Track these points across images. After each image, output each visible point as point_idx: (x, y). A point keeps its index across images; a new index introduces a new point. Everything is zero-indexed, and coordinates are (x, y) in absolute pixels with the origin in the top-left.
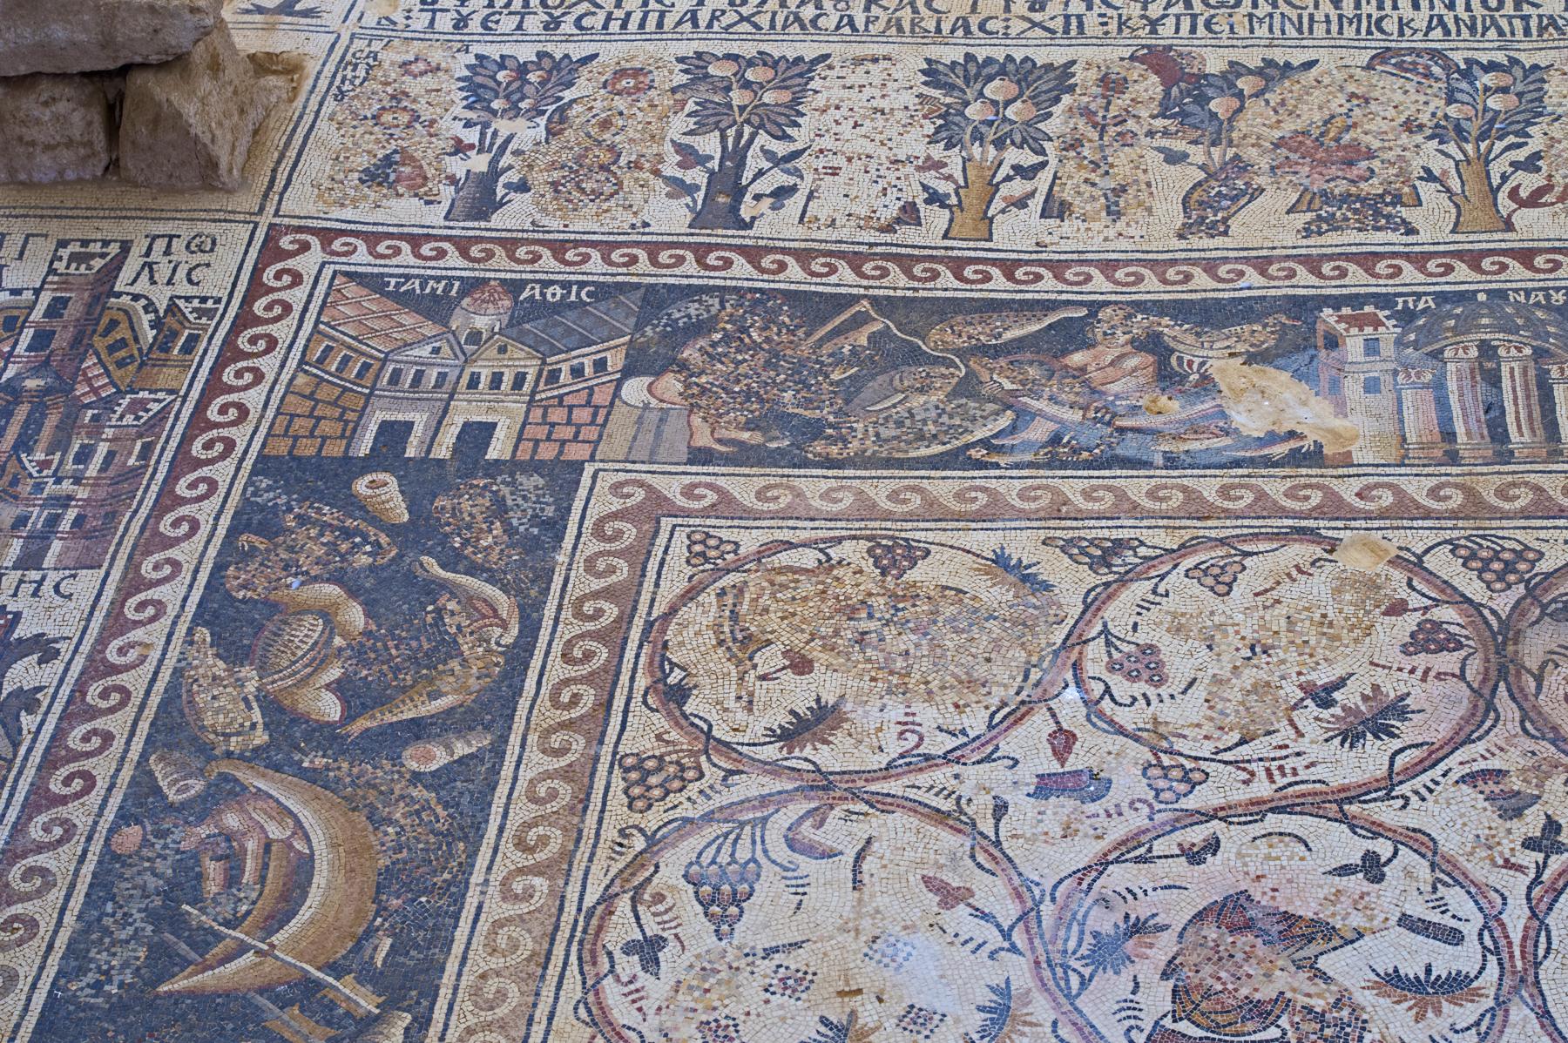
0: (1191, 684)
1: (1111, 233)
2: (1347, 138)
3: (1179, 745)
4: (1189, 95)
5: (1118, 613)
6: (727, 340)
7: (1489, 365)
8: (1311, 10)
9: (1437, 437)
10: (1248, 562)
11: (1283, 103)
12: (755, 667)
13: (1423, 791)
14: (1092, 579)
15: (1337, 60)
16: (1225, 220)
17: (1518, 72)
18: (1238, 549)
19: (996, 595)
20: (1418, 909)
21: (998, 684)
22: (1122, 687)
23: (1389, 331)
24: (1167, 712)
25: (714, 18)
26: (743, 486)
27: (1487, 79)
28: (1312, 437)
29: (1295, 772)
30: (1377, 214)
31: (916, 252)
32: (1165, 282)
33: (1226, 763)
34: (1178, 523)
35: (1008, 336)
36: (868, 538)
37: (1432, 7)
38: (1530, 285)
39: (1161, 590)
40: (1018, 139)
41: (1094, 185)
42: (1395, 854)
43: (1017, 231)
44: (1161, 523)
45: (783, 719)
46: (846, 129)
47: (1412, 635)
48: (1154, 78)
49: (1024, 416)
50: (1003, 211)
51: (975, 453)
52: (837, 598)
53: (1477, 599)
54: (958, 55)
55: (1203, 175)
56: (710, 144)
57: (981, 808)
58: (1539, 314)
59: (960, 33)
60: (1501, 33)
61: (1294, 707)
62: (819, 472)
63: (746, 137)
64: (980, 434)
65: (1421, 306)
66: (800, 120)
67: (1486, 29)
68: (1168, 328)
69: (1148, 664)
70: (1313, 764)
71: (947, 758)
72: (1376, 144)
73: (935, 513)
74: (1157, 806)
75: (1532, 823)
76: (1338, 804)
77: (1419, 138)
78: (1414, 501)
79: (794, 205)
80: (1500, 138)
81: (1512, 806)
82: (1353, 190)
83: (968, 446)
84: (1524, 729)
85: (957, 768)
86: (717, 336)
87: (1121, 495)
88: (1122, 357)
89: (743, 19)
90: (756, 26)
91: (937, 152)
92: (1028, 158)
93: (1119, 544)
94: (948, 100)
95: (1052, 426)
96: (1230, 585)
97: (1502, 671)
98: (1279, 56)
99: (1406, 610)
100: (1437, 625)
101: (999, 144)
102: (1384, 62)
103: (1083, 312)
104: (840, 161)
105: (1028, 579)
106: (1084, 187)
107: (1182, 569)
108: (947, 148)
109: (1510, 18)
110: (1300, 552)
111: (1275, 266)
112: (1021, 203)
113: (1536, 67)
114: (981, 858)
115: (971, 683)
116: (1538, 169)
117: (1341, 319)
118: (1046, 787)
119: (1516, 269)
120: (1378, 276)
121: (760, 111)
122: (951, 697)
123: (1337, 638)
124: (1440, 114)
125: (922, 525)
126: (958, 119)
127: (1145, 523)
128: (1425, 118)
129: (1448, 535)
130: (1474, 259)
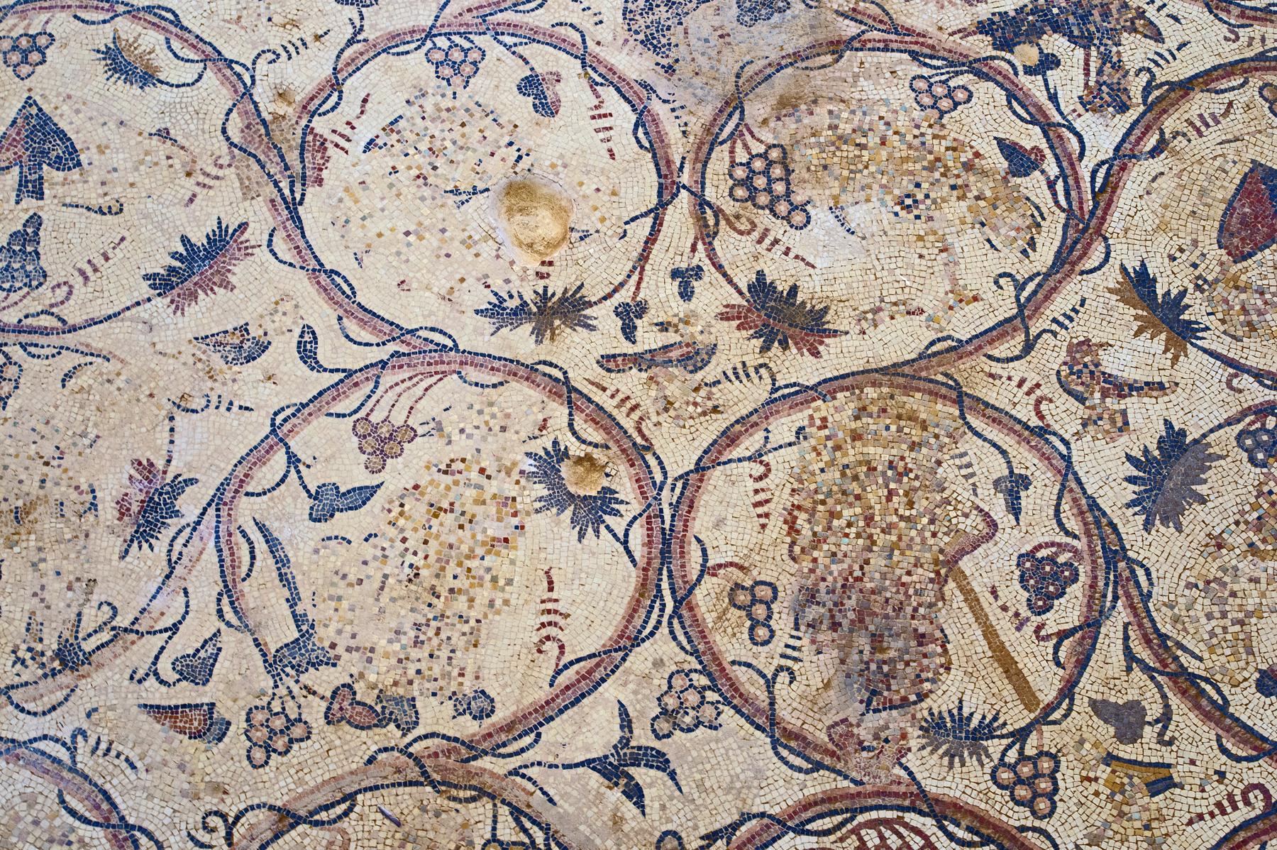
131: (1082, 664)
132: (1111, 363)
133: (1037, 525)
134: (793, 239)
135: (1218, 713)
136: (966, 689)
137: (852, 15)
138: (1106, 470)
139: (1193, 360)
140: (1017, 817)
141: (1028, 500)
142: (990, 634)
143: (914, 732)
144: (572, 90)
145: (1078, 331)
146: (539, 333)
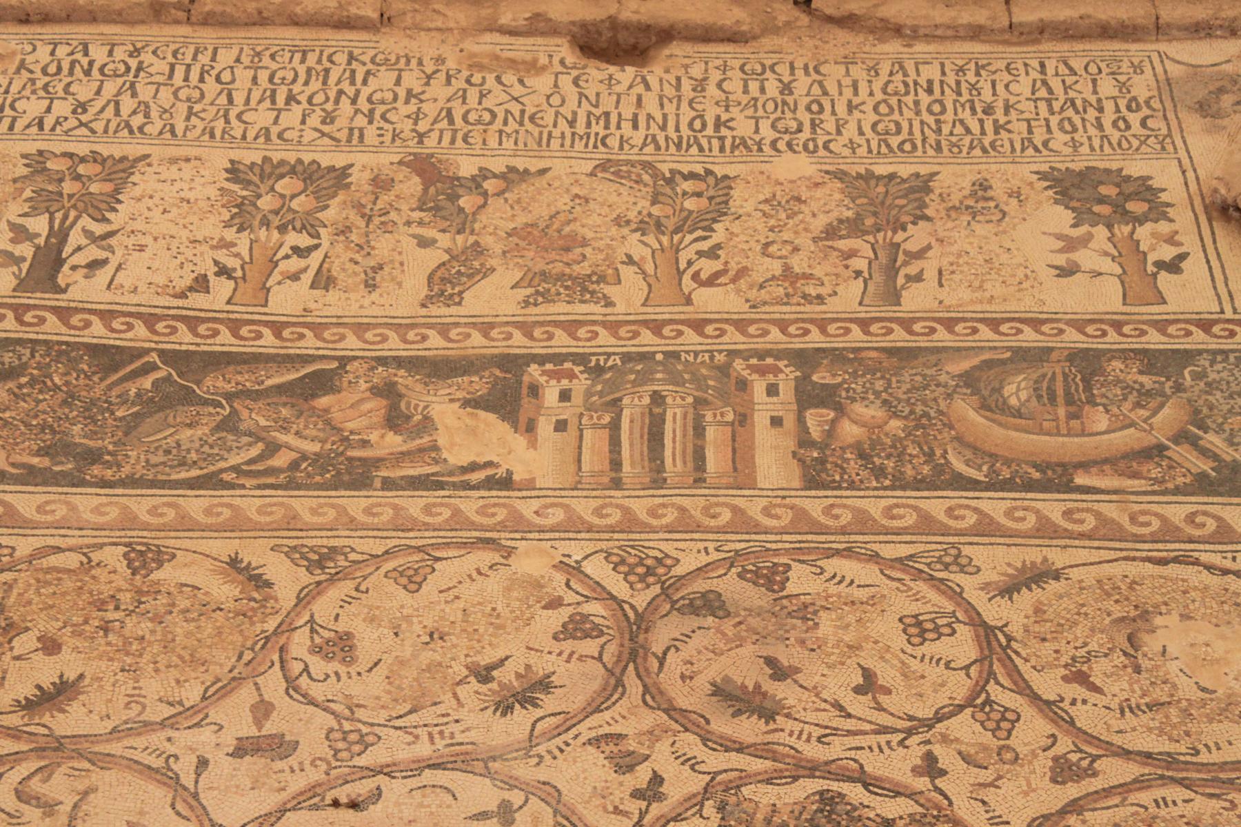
0: (376, 664)
1: (366, 302)
2: (567, 229)
3: (360, 714)
4: (442, 191)
5: (323, 608)
6: (33, 381)
7: (657, 410)
8: (550, 128)
9: (606, 466)
10: (438, 566)
11: (519, 201)
12: (11, 649)
13: (557, 753)
14: (305, 578)
15: (569, 167)
16: (461, 293)
17: (711, 180)
18: (430, 556)
19: (224, 591)
21: (216, 664)
22: (318, 666)
23: (580, 384)
24: (356, 689)
25: (58, 123)
26: (25, 501)
27: (687, 186)
28: (505, 467)
29: (452, 736)
30: (585, 290)
31: (202, 314)
32: (405, 341)
33: (396, 728)
34: (385, 534)
35: (269, 383)
36: (126, 545)
37: (648, 128)
38: (699, 348)
39: (363, 588)
40: (298, 225)
41: (356, 263)
42: (526, 801)
43: (288, 299)
44: (371, 533)
45: (28, 691)
46: (156, 214)
47: (564, 625)
48: (417, 179)
49: (273, 448)
50: (279, 283)
51: (227, 477)
52: (91, 593)
53: (621, 596)
54: (256, 157)
55: (447, 257)
56: (39, 225)
57: (185, 768)
58: (704, 371)
59: (262, 140)
60: (701, 149)
61: (458, 684)
62: (93, 490)
63: (71, 219)
64: (234, 460)
65: (610, 363)
66: (118, 206)
67: (689, 146)
68: (402, 378)
69: (341, 646)
70: (468, 729)
71: (162, 724)
72: (590, 235)
73: (186, 525)
74: (334, 763)
75: (642, 775)
77: (625, 231)
78: (580, 518)
79: (103, 275)
80: (690, 232)
82: (567, 271)
83: (222, 471)
84: (645, 702)
85: (171, 733)
86: (24, 380)
87: (342, 511)
88: (362, 401)
89: (82, 124)
90: (93, 131)
91: (230, 234)
92: (304, 241)
93: (333, 549)
94: (245, 193)
95: (294, 455)
96: (420, 584)
97: (633, 654)
98: (520, 163)
99: (561, 605)
100: (585, 618)
101: (282, 229)
102: (604, 170)
103: (335, 365)
104: (148, 240)
106: (349, 265)
107: (383, 571)
108: (239, 231)
109: (709, 138)
110: (485, 557)
111: (496, 331)
112: (295, 277)
113: (726, 177)
114: (180, 807)
115: (194, 661)
116: (718, 257)
117: (544, 373)
119: (690, 336)
120: (579, 339)
121: (86, 199)
122: (174, 673)
123: (502, 627)
124: (645, 212)
125: (173, 534)
126: (250, 208)
127: (359, 533)
128: (632, 215)
129: (604, 545)
130: (656, 327)
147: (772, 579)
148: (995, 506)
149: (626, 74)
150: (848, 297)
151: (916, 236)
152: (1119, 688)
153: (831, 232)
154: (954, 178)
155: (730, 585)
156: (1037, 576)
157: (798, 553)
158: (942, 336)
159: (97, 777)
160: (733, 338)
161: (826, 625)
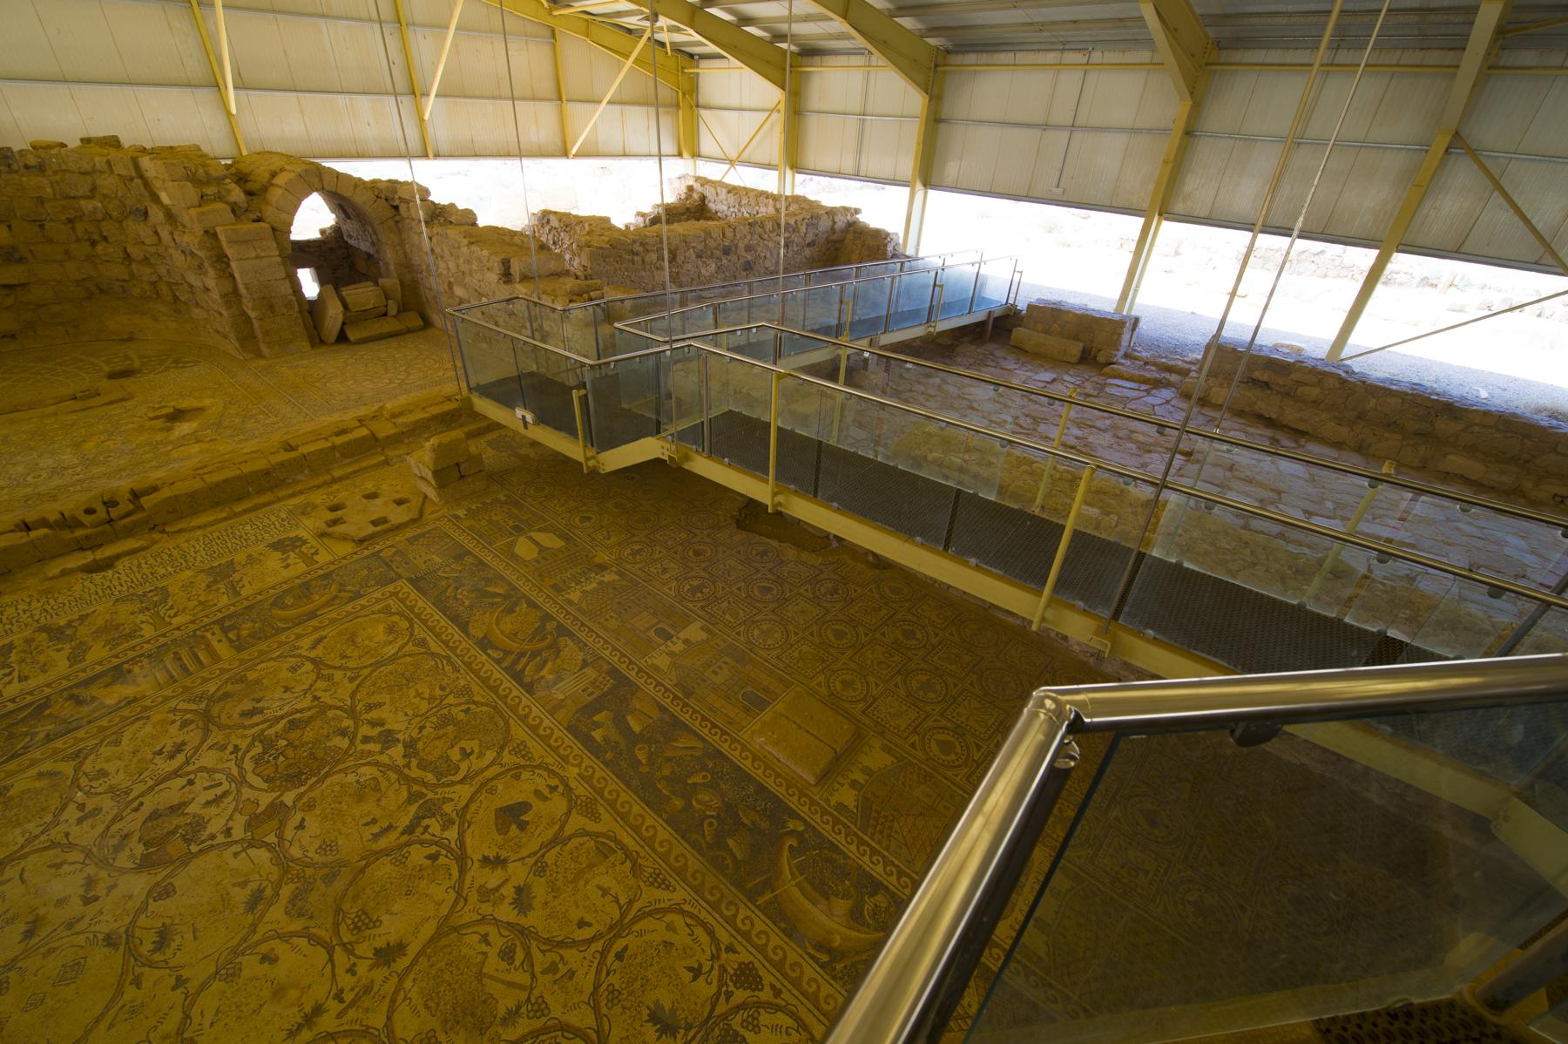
4: (56, 634)
20: (207, 784)
22: (95, 784)
23: (146, 661)
24: (113, 781)
49: (33, 735)
68: (75, 691)
69: (103, 773)
75: (230, 748)
76: (175, 774)
81: (224, 748)
97: (207, 718)
105: (51, 774)
110: (140, 723)
115: (43, 809)
118: (80, 821)
119: (177, 633)
130: (164, 635)
131: (532, 965)
132: (490, 885)
133: (498, 942)
134: (380, 930)
135: (574, 944)
136: (506, 1002)
137: (363, 858)
138: (506, 913)
139: (511, 866)
140: (540, 1023)
141: (490, 939)
142: (503, 982)
143: (501, 1030)
144: (280, 948)
145: (477, 885)
146: (310, 1028)
147: (242, 679)
148: (299, 630)
149: (110, 573)
150: (224, 600)
151: (237, 576)
152: (356, 654)
153: (208, 586)
154: (240, 557)
155: (229, 688)
156: (320, 640)
157: (247, 670)
158: (259, 598)
159: (23, 863)
160: (192, 627)
161: (265, 682)
